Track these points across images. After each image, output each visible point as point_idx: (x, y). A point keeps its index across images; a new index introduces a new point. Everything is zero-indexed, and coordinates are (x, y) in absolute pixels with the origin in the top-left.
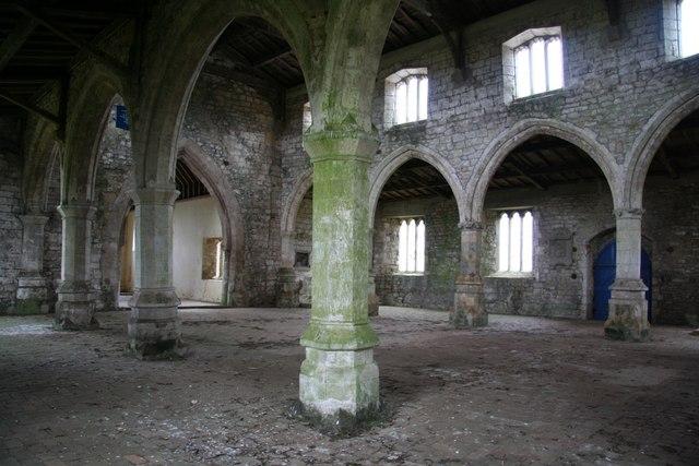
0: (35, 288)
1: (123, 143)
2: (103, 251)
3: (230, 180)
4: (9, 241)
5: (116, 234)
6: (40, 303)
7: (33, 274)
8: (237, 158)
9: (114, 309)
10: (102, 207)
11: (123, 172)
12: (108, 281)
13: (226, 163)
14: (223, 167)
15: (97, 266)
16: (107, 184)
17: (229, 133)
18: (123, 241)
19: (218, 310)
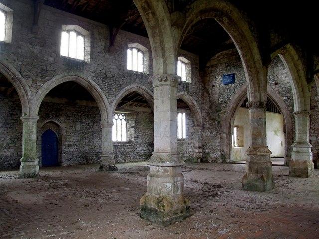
0: (196, 153)
1: (226, 91)
2: (221, 138)
3: (279, 92)
4: (192, 137)
5: (226, 130)
6: (198, 158)
7: (195, 149)
8: (283, 79)
9: (226, 163)
10: (219, 120)
11: (226, 103)
12: (223, 151)
13: (276, 84)
14: (274, 86)
15: (219, 144)
16: (221, 110)
17: (277, 66)
18: (230, 134)
19: (280, 167)
